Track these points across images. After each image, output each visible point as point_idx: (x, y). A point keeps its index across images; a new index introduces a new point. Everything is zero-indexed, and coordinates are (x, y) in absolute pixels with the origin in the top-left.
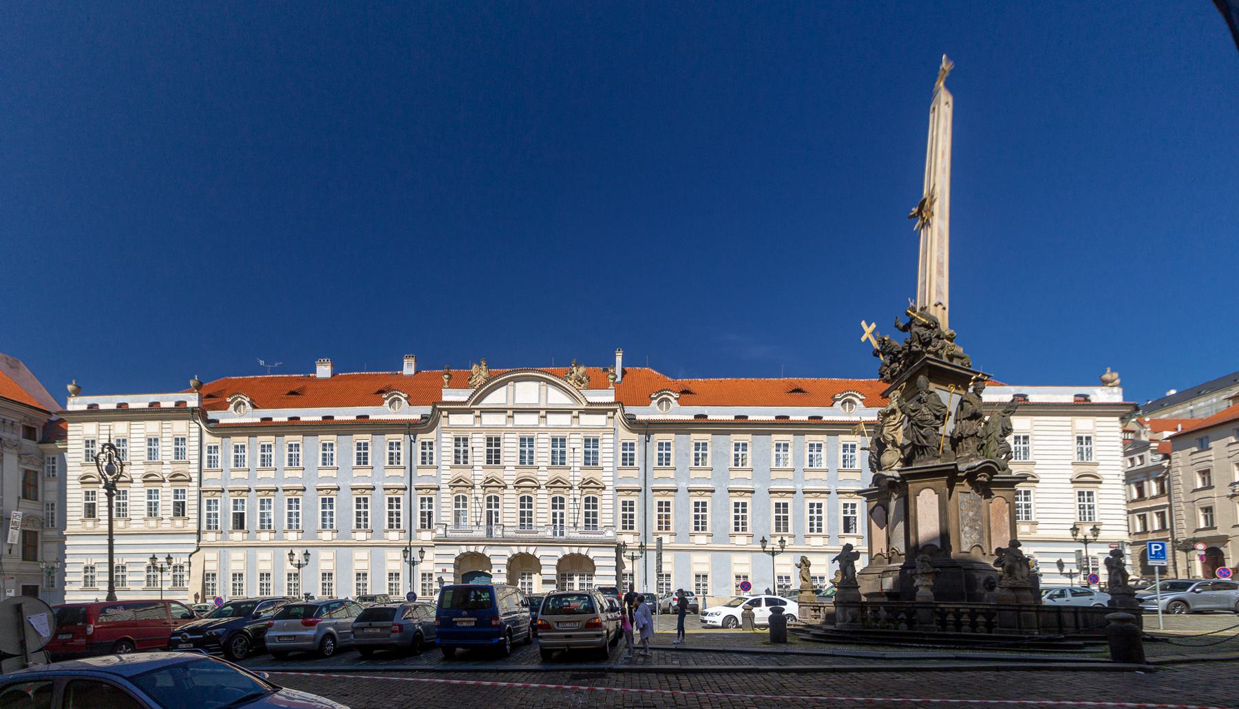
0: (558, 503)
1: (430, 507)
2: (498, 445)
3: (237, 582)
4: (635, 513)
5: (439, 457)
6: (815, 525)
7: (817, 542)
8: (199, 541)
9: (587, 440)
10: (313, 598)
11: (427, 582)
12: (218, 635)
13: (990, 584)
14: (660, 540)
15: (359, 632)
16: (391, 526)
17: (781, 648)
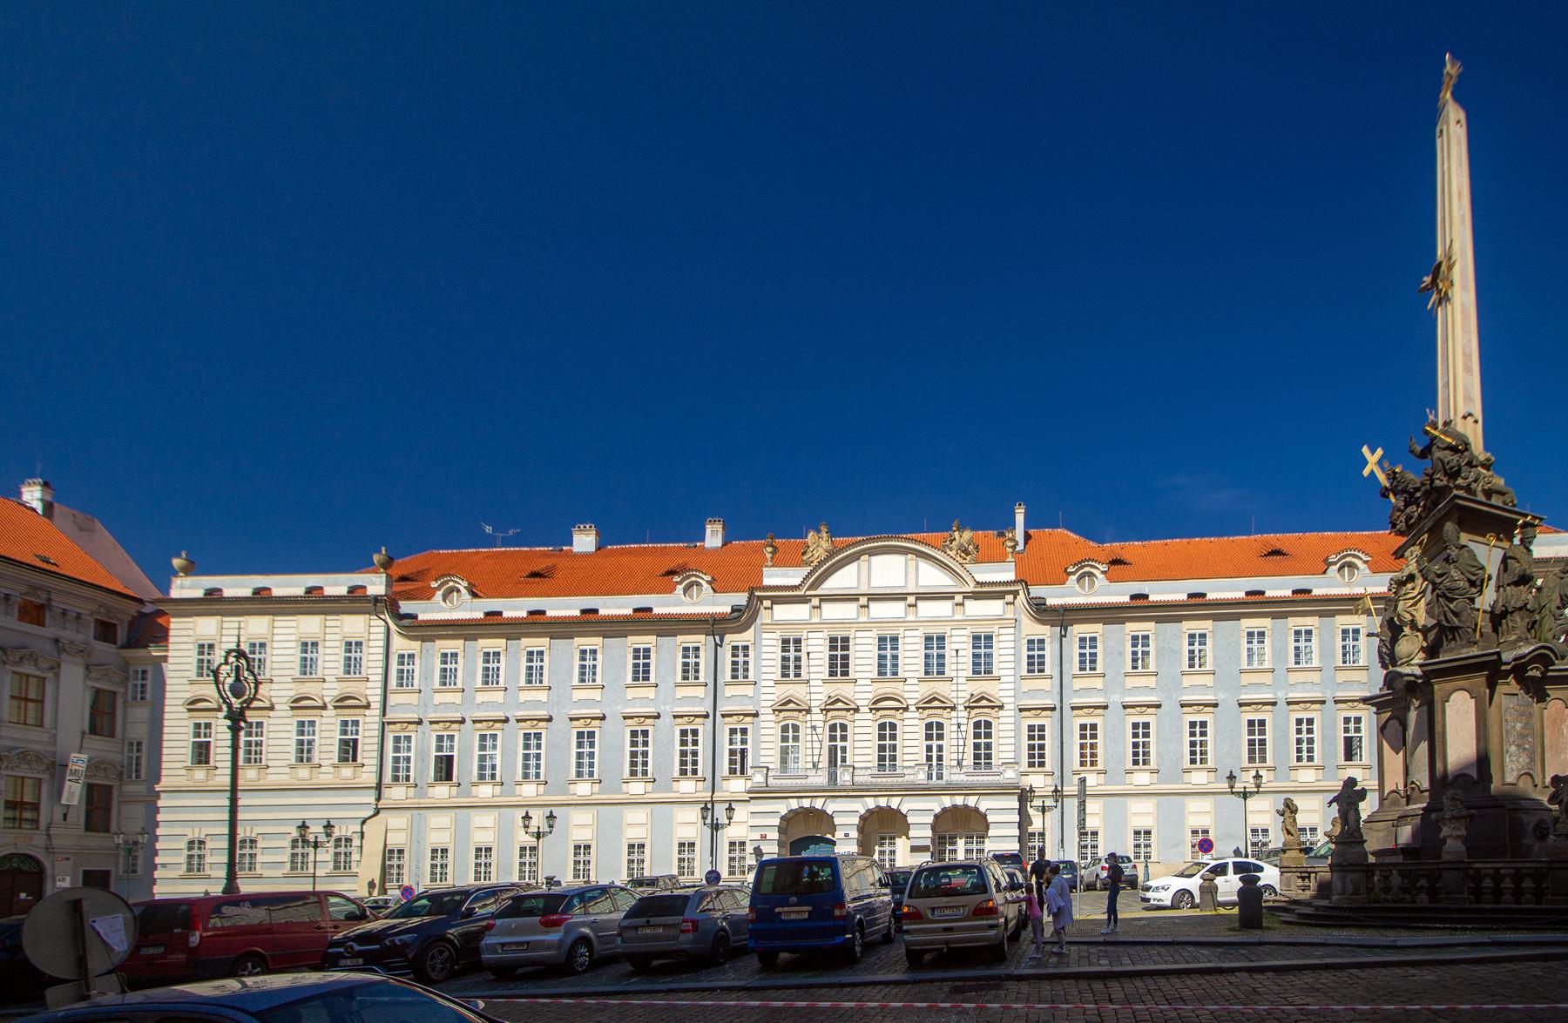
0: (934, 731)
1: (744, 742)
2: (846, 648)
3: (439, 861)
4: (1047, 742)
5: (758, 667)
6: (1305, 751)
7: (1307, 776)
8: (379, 799)
9: (976, 638)
10: (558, 883)
11: (737, 854)
12: (405, 945)
13: (1542, 831)
14: (1083, 781)
15: (630, 934)
16: (683, 772)
17: (1254, 936)
